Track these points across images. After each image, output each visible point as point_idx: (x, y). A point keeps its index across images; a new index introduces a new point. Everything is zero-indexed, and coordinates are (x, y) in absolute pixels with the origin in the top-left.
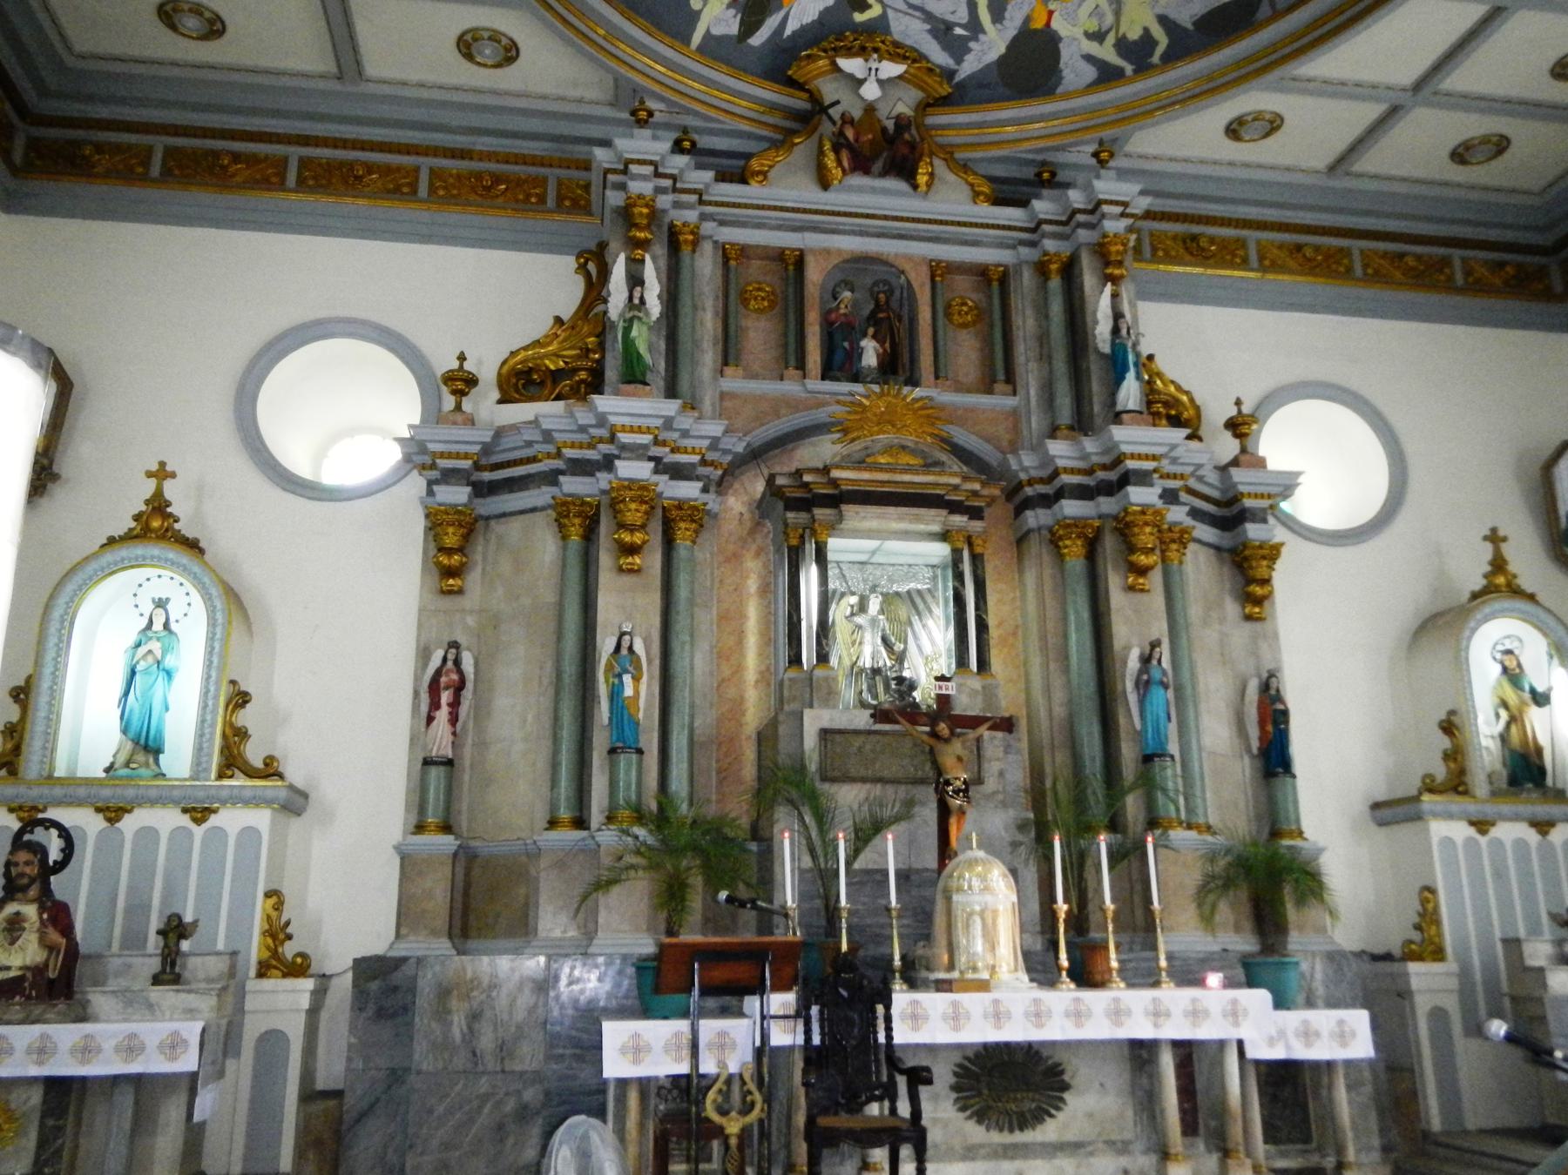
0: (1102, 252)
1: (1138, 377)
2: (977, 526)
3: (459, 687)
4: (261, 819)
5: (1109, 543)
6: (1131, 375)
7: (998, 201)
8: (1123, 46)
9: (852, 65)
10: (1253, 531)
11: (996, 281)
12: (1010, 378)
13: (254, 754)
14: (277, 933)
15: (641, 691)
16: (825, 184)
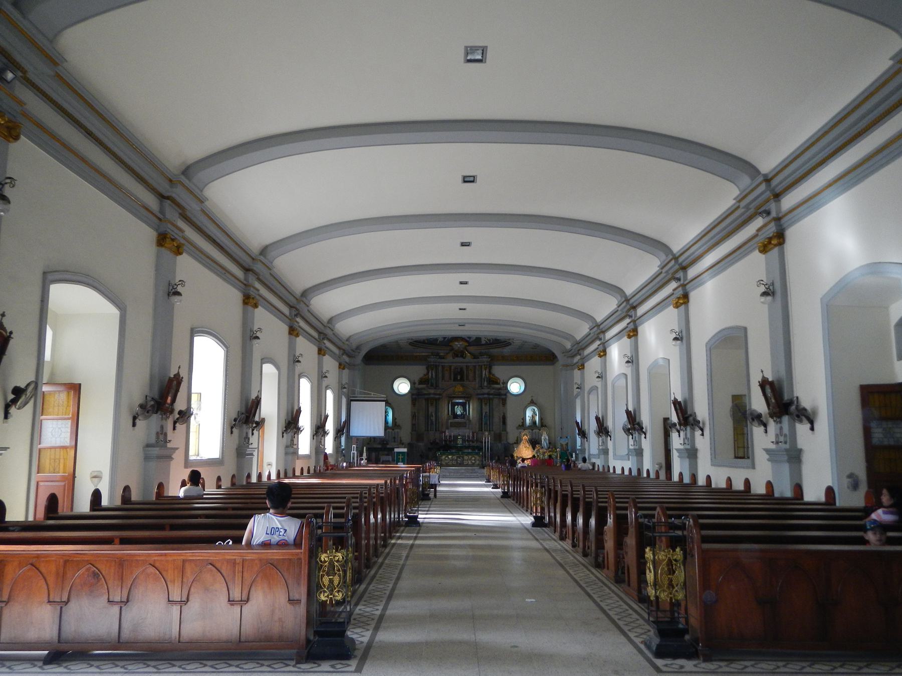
0: (484, 365)
1: (487, 382)
2: (468, 399)
3: (416, 417)
4: (399, 430)
5: (483, 401)
6: (486, 382)
7: (474, 358)
8: (488, 339)
9: (457, 343)
10: (503, 397)
11: (475, 366)
12: (475, 379)
13: (397, 424)
14: (401, 441)
15: (434, 419)
16: (453, 358)
